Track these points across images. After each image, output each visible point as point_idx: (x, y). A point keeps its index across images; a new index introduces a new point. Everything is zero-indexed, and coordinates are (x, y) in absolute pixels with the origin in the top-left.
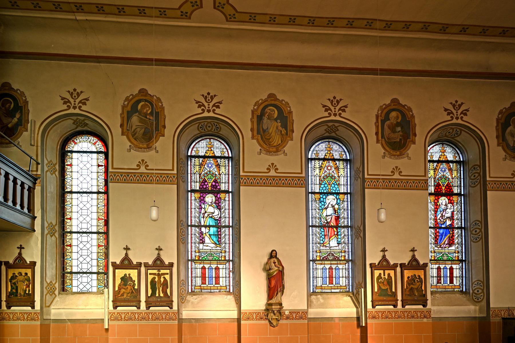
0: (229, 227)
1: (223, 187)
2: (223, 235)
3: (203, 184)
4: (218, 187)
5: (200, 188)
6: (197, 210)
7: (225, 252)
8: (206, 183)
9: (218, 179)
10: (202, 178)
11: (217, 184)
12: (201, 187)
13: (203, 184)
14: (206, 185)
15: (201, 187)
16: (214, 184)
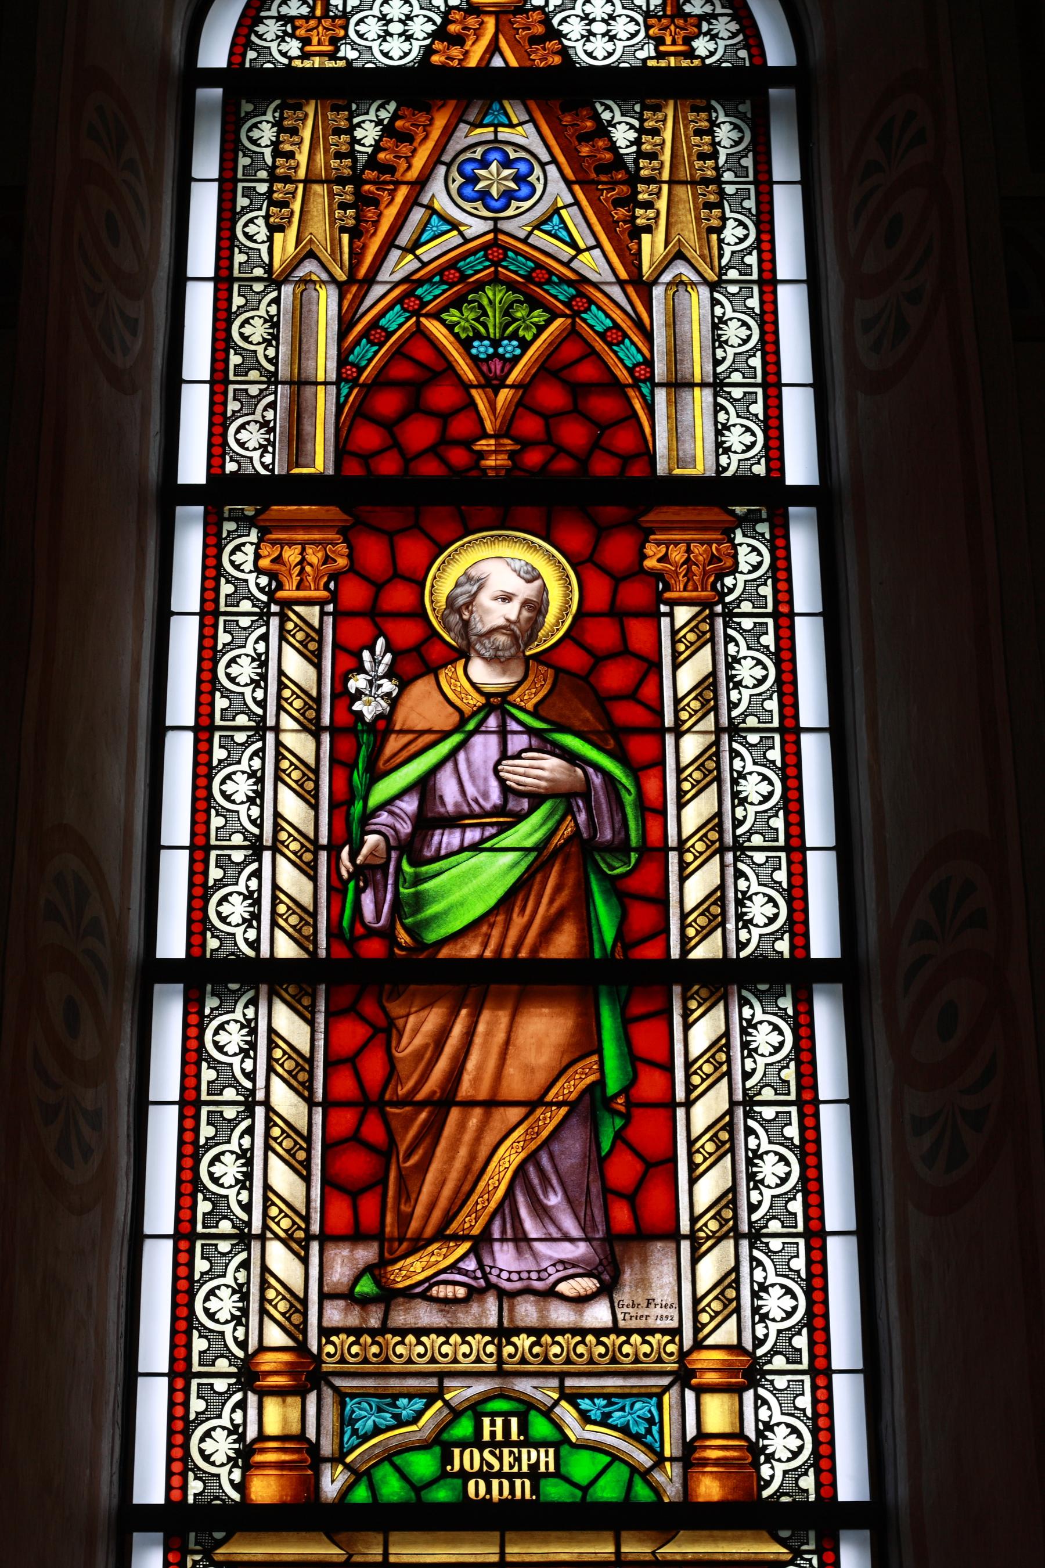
0: (788, 976)
1: (693, 437)
2: (707, 1110)
3: (388, 403)
4: (623, 440)
5: (341, 451)
6: (300, 744)
7: (747, 1373)
8: (441, 397)
9: (614, 335)
10: (375, 333)
11: (603, 406)
12: (369, 438)
13: (388, 403)
14: (444, 417)
15: (369, 438)
16: (552, 396)
